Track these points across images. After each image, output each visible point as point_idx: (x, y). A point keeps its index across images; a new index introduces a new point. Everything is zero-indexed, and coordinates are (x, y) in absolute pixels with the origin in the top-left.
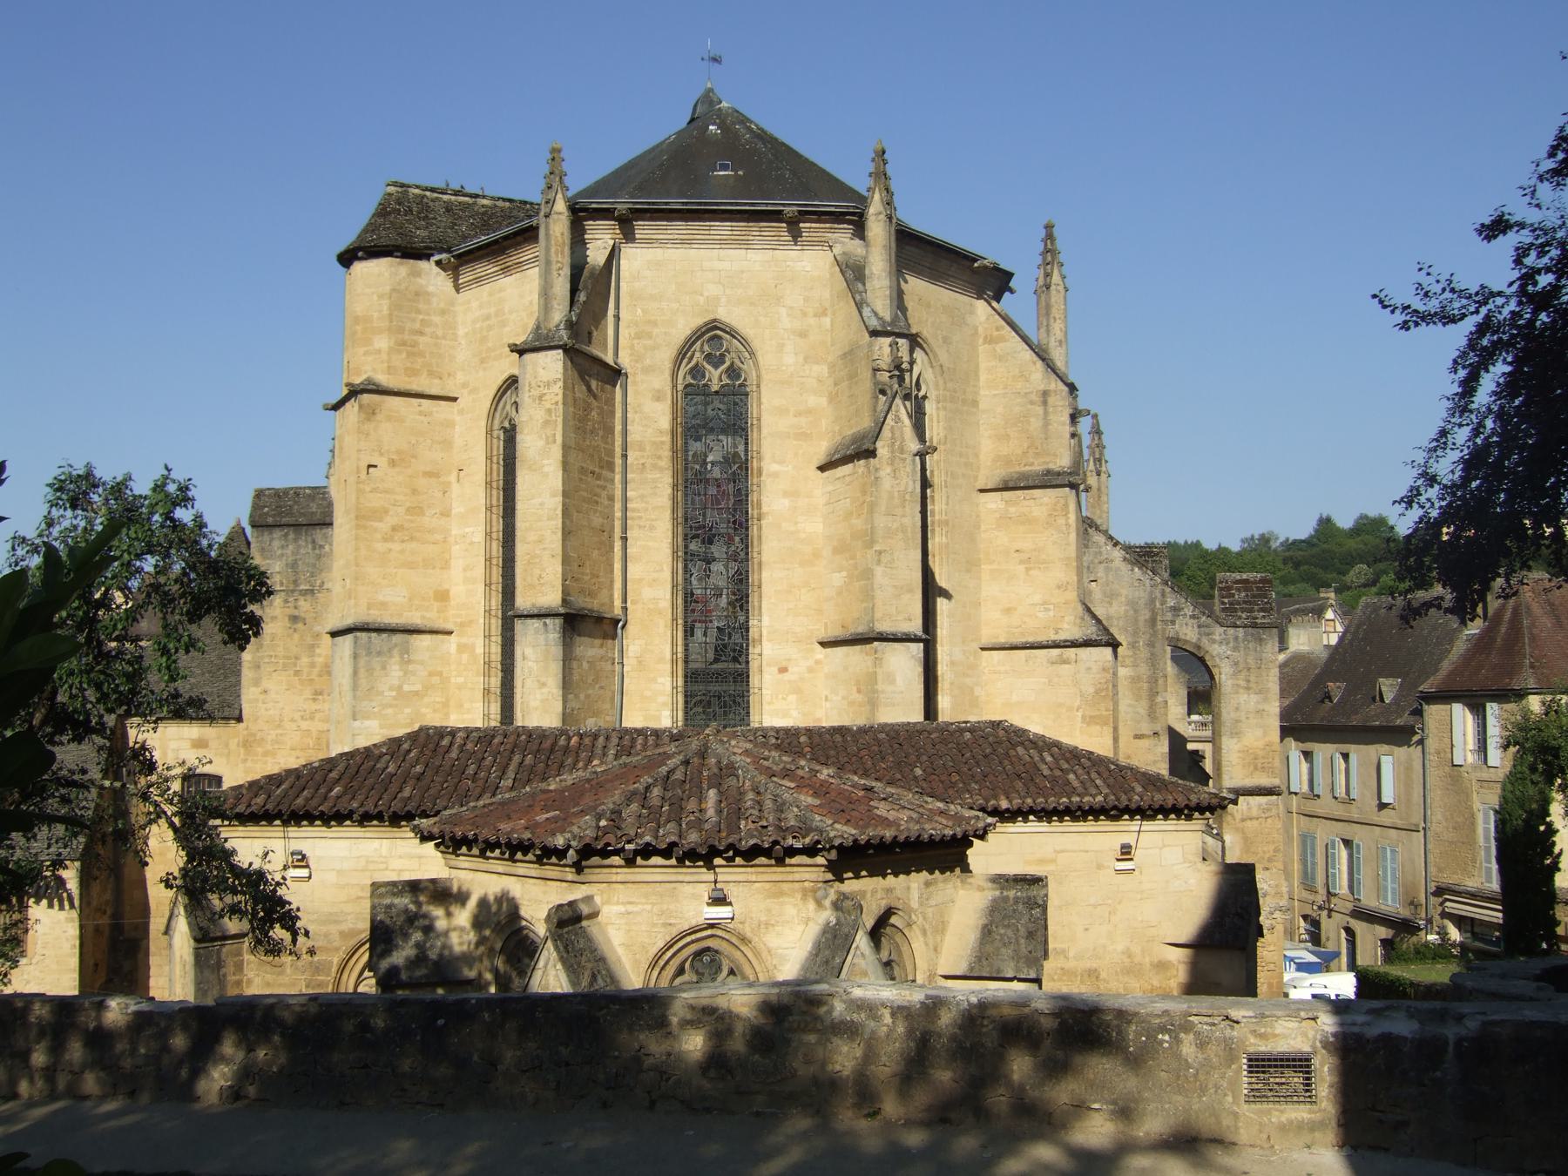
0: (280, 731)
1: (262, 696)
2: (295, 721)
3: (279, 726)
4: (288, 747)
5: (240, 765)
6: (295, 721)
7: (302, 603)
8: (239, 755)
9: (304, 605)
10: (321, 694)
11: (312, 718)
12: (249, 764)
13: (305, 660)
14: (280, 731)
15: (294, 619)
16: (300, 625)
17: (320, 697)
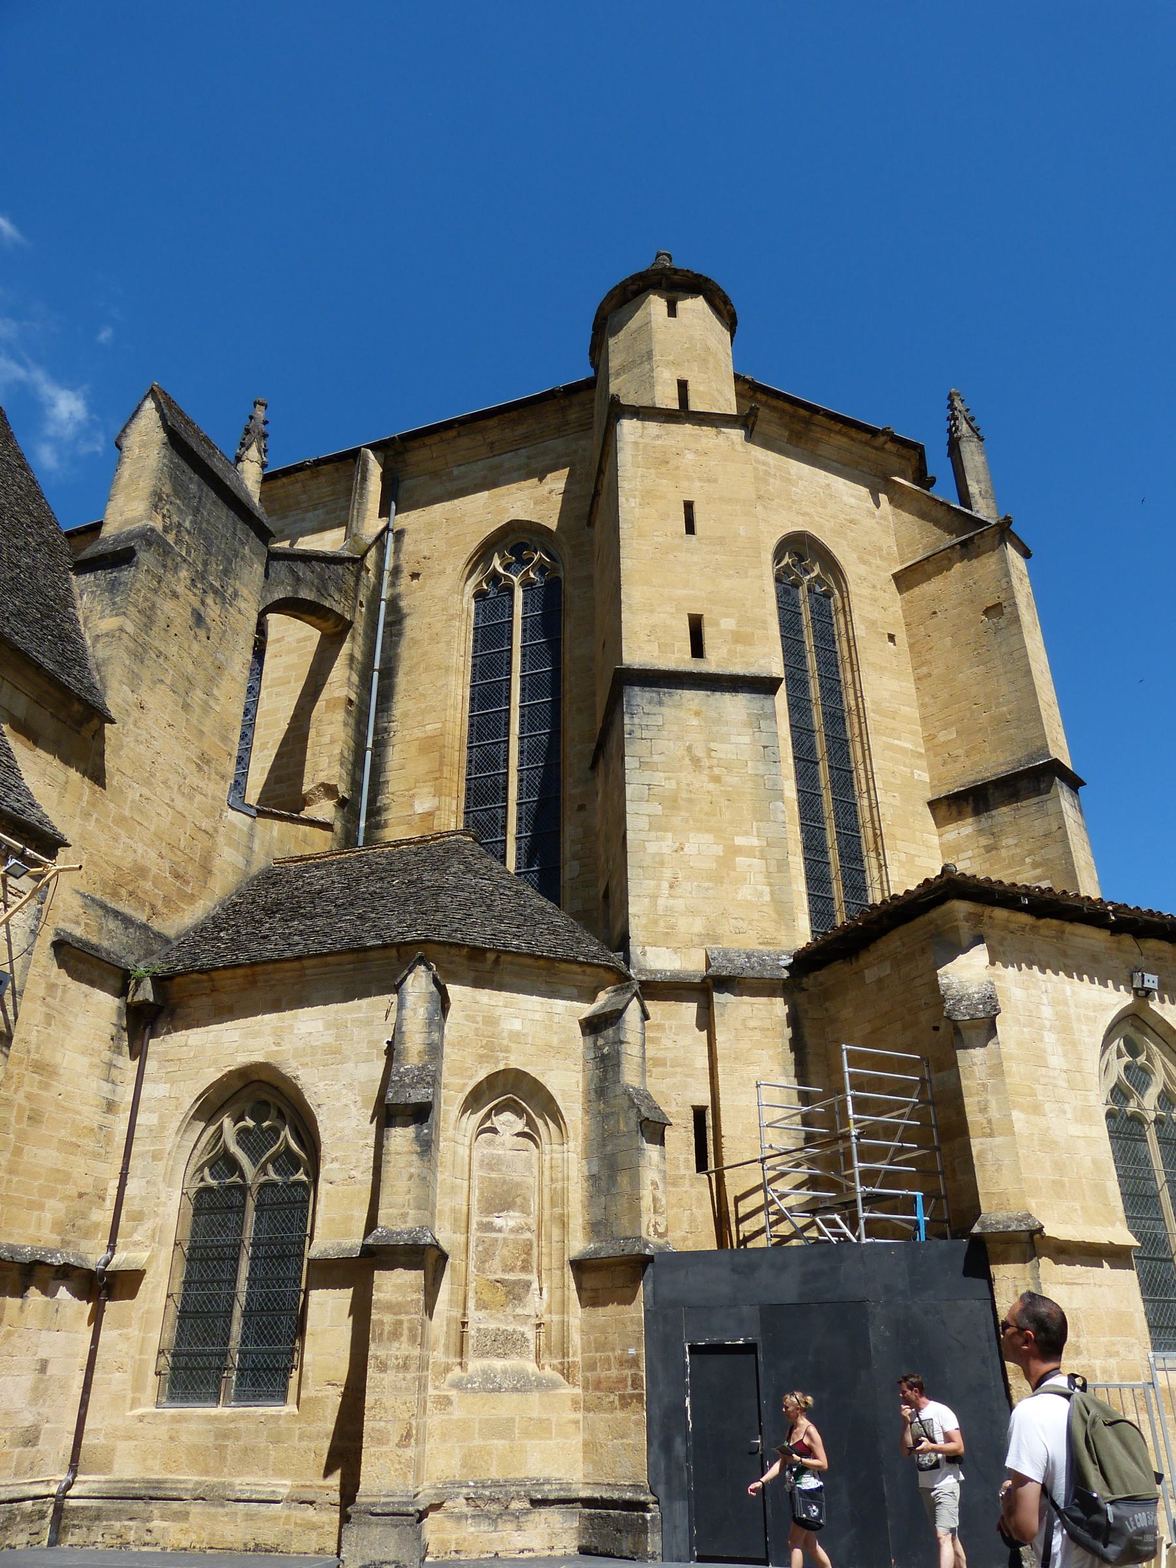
0: (146, 792)
1: (136, 713)
2: (169, 787)
3: (148, 783)
4: (152, 829)
5: (78, 820)
6: (169, 787)
7: (209, 601)
8: (80, 798)
9: (213, 610)
10: (208, 762)
11: (191, 798)
12: (91, 826)
13: (198, 695)
14: (146, 792)
15: (199, 619)
16: (202, 634)
17: (206, 768)
